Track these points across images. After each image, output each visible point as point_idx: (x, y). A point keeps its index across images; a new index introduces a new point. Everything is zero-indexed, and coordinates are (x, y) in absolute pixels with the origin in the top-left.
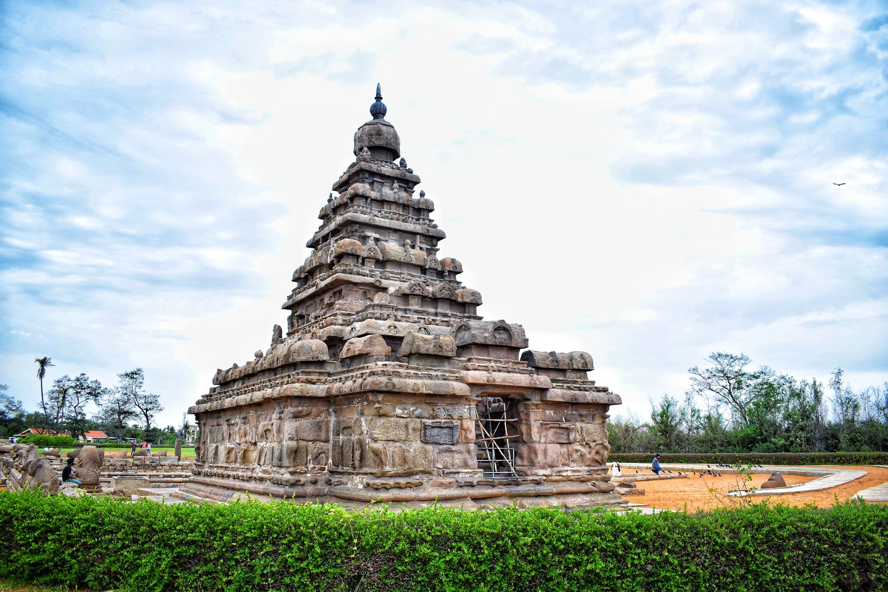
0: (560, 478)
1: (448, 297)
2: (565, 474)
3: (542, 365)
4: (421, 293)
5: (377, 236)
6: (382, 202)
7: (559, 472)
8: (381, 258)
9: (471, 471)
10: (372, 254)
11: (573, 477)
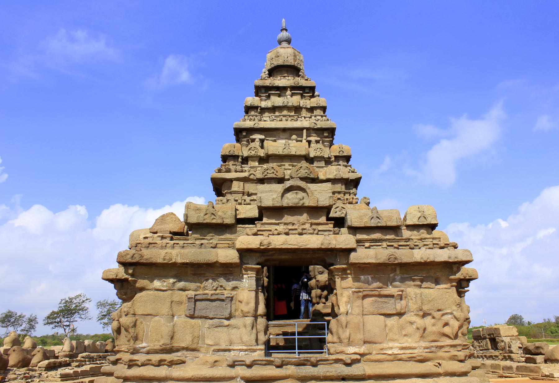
0: (384, 356)
1: (306, 175)
2: (390, 352)
3: (356, 224)
4: (275, 176)
5: (262, 137)
6: (273, 109)
7: (382, 349)
8: (262, 155)
9: (245, 348)
10: (253, 153)
11: (403, 356)
